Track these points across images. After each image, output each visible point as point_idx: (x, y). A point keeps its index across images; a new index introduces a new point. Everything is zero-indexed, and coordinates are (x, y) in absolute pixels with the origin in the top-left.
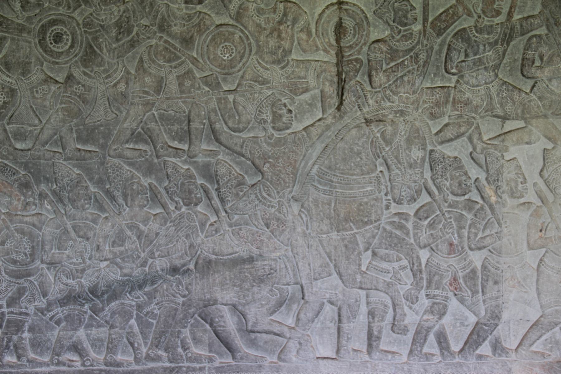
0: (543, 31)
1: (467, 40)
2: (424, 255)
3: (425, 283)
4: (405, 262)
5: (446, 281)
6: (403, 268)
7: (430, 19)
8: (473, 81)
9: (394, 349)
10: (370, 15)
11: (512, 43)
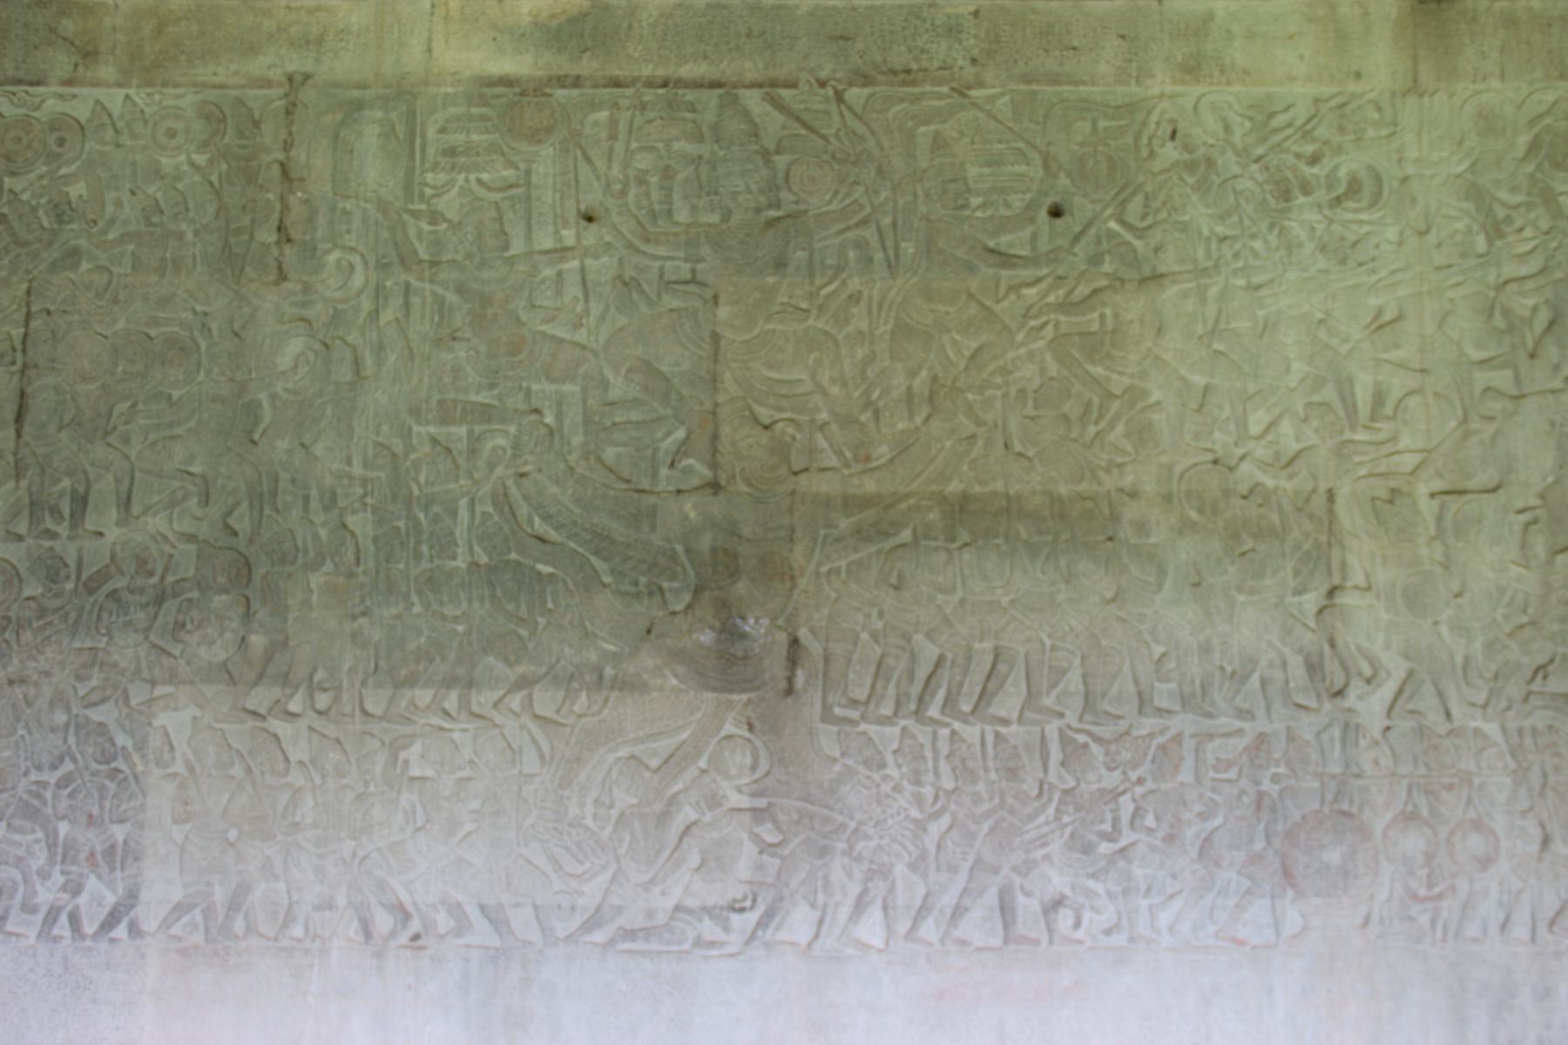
0: (195, 594)
1: (119, 601)
2: (63, 828)
3: (59, 858)
4: (40, 835)
5: (82, 856)
6: (37, 841)
7: (84, 577)
8: (122, 643)
9: (21, 930)
10: (22, 571)
11: (165, 606)
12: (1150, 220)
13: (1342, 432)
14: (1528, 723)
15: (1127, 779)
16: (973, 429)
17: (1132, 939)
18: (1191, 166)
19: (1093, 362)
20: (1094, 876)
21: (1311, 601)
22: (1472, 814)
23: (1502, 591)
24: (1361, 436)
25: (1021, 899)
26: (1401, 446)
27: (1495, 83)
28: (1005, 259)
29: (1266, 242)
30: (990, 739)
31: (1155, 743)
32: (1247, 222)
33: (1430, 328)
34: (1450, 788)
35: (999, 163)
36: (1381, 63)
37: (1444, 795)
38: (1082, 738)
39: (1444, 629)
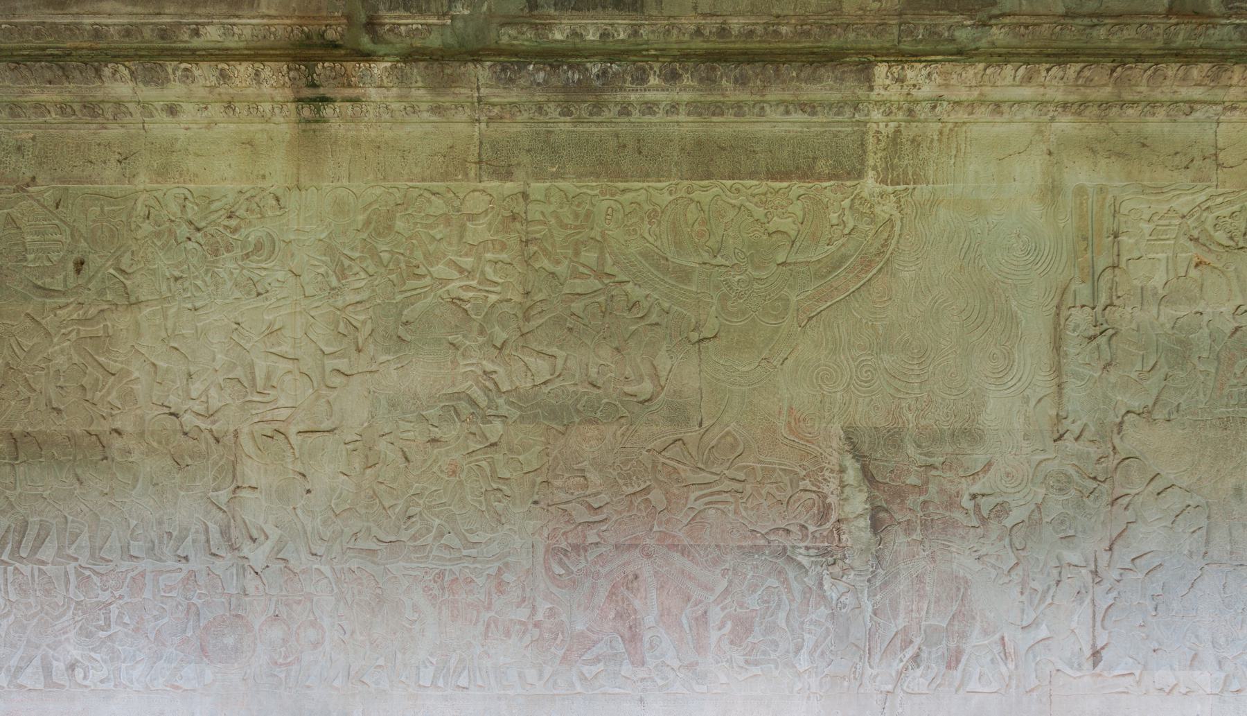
12: (135, 268)
13: (245, 396)
14: (346, 566)
15: (114, 596)
16: (29, 394)
17: (115, 686)
18: (158, 235)
19: (98, 354)
20: (93, 650)
21: (223, 496)
22: (312, 618)
23: (333, 490)
24: (257, 398)
25: (55, 663)
26: (280, 404)
27: (345, 182)
28: (47, 292)
29: (204, 281)
30: (36, 573)
31: (129, 576)
32: (193, 269)
33: (300, 334)
34: (299, 602)
35: (44, 234)
36: (277, 170)
37: (295, 606)
38: (87, 573)
39: (299, 512)
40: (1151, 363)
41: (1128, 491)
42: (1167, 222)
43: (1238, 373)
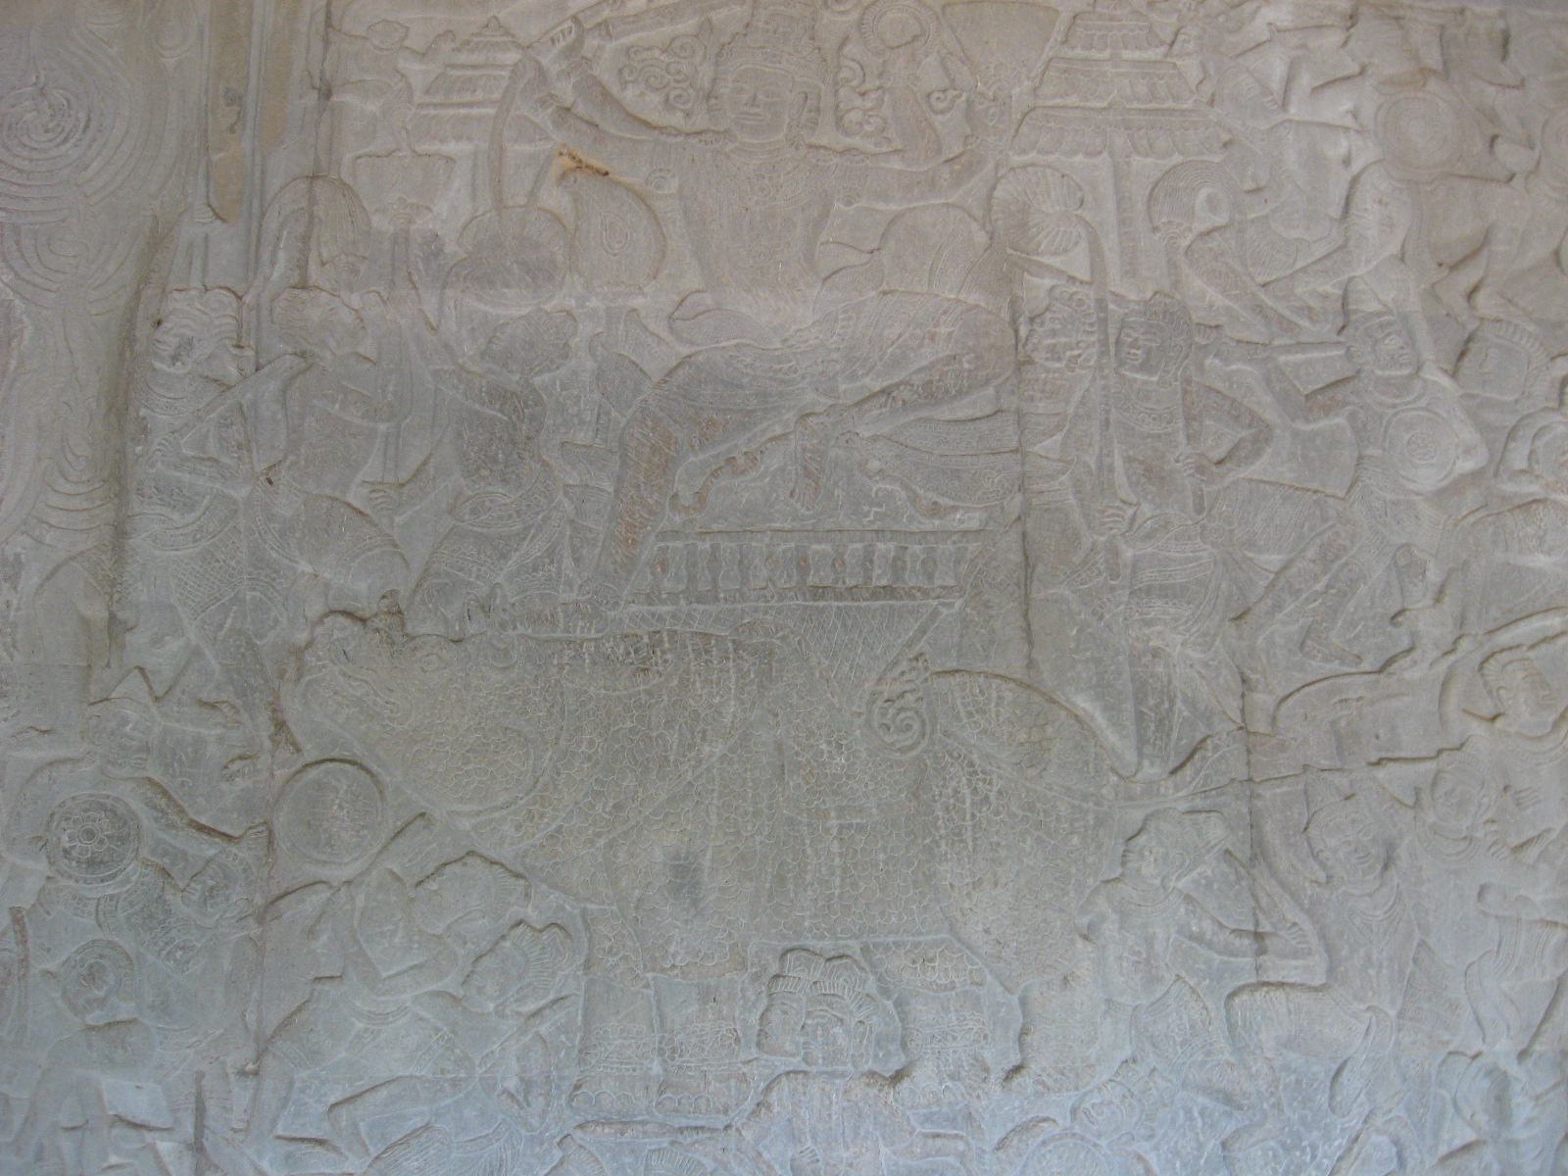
40: (414, 459)
41: (324, 873)
42: (477, 58)
43: (687, 498)
